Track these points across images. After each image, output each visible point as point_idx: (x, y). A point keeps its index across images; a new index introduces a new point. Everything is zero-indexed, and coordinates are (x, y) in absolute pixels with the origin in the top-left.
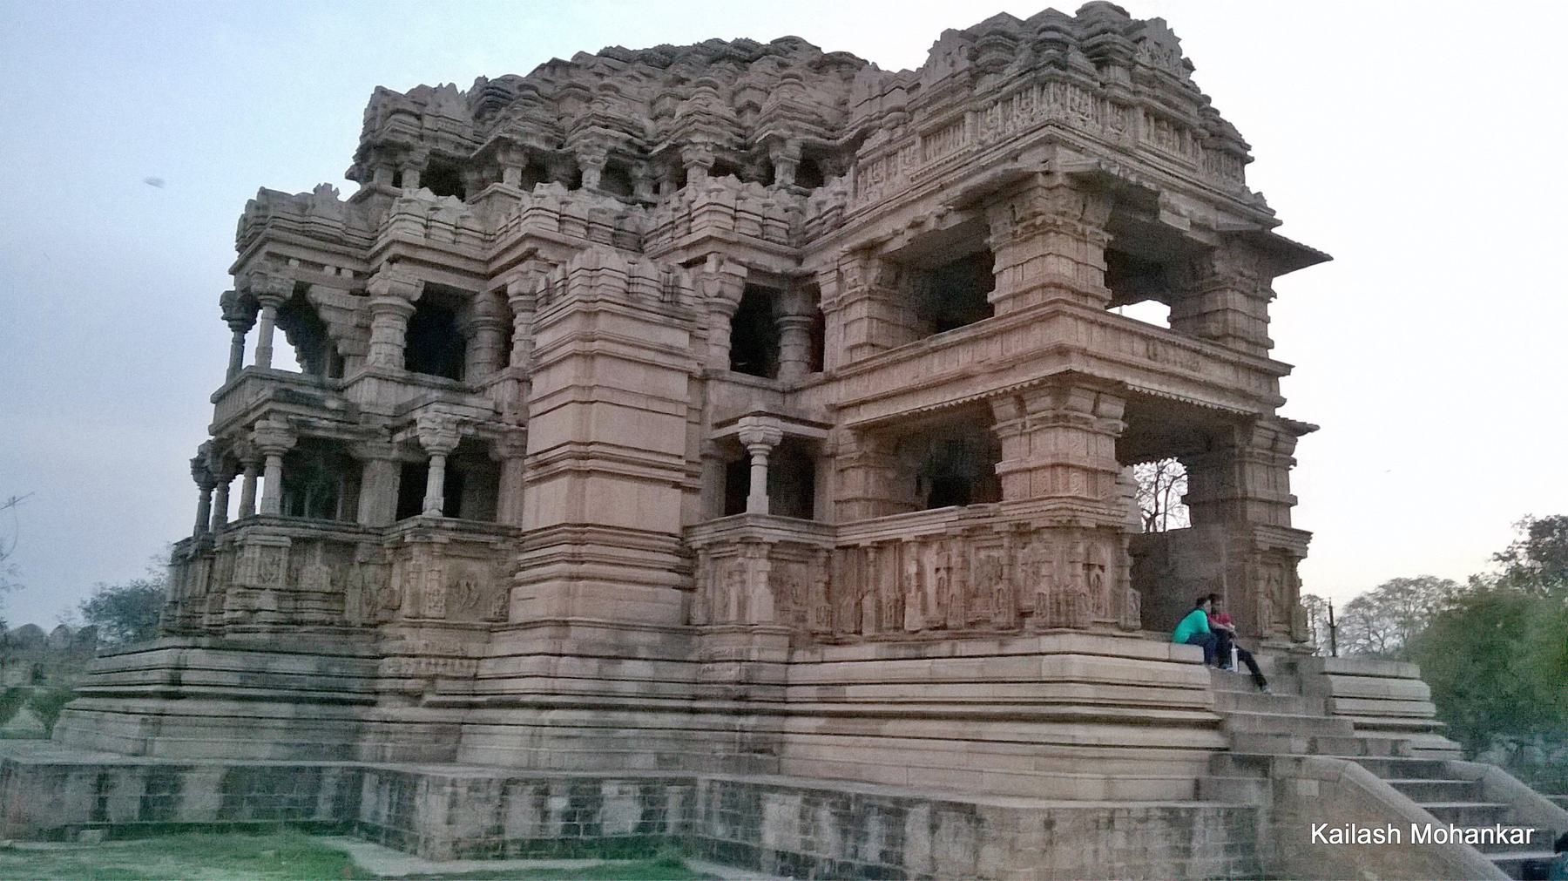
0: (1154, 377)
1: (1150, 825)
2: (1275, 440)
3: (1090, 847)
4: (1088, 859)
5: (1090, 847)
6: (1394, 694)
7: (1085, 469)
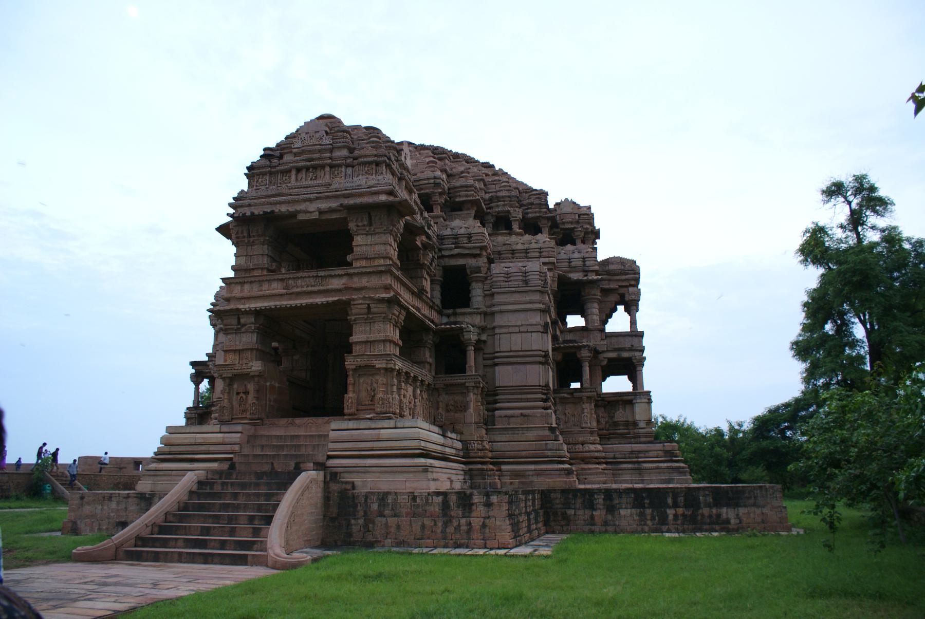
1: (130, 500)
2: (369, 308)
3: (100, 507)
4: (98, 511)
5: (100, 507)
6: (382, 437)
7: (235, 351)
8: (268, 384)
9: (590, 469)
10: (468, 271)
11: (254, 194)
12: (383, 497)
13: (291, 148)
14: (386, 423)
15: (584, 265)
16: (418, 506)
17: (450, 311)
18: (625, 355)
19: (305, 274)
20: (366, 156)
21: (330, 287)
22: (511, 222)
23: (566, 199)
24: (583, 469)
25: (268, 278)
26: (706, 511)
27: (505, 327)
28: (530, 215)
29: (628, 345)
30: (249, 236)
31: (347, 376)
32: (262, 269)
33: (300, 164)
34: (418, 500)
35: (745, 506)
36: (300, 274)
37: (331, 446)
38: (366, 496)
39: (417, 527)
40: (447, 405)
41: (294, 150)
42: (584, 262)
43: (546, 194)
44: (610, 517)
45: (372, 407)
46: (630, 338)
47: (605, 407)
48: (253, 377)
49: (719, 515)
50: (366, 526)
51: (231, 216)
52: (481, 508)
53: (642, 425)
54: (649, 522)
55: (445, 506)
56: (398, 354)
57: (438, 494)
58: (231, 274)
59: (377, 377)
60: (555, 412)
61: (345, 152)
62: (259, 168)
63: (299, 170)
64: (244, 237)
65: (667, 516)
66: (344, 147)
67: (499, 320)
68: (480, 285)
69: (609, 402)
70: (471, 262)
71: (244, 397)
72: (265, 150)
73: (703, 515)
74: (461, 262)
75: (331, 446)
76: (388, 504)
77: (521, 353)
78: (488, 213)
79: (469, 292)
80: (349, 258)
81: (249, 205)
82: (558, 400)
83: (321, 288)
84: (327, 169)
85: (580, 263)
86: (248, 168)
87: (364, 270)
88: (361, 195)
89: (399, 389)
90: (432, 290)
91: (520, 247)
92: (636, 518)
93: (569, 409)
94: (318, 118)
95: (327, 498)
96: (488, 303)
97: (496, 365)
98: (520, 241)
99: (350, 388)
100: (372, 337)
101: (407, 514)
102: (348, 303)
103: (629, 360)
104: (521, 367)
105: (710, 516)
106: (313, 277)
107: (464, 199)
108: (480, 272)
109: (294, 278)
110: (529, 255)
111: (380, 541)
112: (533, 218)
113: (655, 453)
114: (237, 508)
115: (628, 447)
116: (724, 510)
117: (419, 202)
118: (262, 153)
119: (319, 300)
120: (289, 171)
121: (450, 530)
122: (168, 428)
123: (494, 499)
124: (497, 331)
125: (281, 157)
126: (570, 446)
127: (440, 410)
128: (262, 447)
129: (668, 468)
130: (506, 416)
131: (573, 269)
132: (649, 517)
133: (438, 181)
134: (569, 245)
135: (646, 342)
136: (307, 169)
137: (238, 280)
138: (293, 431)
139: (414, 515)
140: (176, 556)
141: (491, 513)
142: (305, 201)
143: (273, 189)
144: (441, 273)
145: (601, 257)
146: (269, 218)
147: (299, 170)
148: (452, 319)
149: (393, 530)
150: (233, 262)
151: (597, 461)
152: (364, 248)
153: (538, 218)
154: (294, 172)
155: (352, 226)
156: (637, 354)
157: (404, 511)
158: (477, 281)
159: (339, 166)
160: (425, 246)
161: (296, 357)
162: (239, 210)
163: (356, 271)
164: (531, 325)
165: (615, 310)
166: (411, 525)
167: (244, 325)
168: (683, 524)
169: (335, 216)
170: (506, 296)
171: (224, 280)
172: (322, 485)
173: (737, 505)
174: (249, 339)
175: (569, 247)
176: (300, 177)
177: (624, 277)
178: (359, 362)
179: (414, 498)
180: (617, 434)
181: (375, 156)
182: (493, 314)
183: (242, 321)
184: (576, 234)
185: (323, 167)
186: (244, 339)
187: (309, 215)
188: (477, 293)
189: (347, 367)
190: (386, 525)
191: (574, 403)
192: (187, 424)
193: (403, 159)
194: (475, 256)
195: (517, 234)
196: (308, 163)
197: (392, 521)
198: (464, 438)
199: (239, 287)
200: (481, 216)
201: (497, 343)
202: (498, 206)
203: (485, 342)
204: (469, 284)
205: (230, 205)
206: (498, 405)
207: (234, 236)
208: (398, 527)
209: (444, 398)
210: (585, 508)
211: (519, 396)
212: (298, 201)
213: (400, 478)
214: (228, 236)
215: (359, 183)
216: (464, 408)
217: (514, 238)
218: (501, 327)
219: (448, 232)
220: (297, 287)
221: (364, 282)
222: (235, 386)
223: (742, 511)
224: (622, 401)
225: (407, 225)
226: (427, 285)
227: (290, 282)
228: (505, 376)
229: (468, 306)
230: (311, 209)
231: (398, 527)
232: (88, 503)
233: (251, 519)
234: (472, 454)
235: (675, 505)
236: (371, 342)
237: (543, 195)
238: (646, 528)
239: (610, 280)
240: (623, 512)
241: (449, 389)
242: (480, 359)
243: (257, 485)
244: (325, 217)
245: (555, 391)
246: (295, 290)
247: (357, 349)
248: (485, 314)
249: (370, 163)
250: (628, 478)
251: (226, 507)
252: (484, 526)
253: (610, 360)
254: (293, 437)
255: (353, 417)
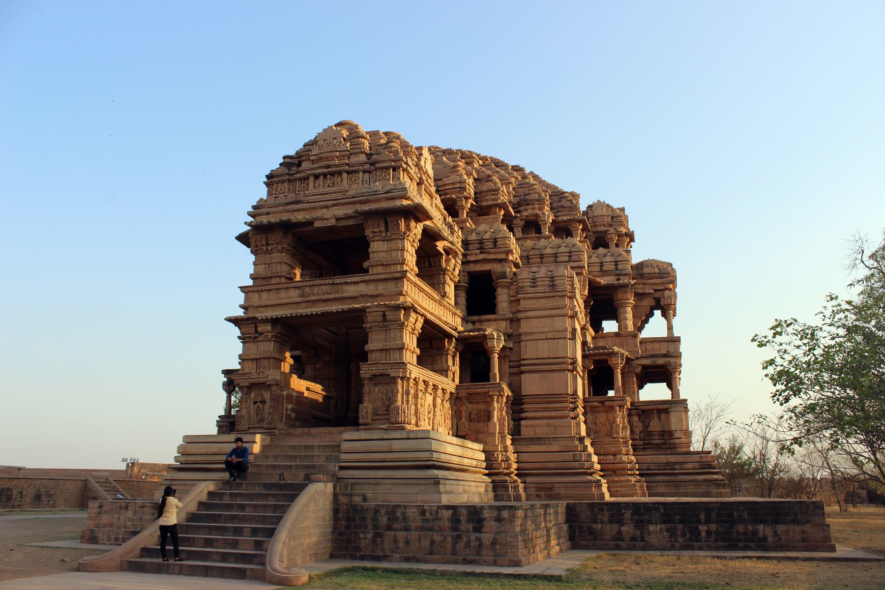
0: (303, 305)
1: (145, 509)
3: (117, 516)
7: (252, 359)
8: (285, 393)
9: (622, 481)
10: (493, 276)
11: (272, 201)
12: (392, 511)
13: (309, 155)
14: (398, 434)
15: (617, 269)
16: (427, 520)
17: (476, 318)
18: (660, 361)
19: (322, 282)
20: (383, 161)
21: (346, 295)
22: (540, 226)
23: (599, 201)
24: (614, 482)
25: (285, 286)
26: (740, 528)
27: (531, 334)
28: (560, 218)
29: (664, 352)
30: (268, 245)
31: (363, 385)
32: (280, 277)
33: (317, 171)
34: (427, 515)
35: (784, 522)
36: (317, 282)
37: (343, 456)
38: (376, 511)
39: (426, 544)
40: (470, 415)
41: (312, 158)
42: (616, 265)
43: (578, 196)
44: (638, 532)
45: (387, 417)
46: (666, 344)
47: (639, 416)
48: (269, 386)
49: (755, 532)
50: (374, 541)
51: (249, 224)
52: (493, 523)
53: (677, 435)
54: (680, 540)
55: (455, 520)
56: (415, 362)
57: (448, 507)
58: (250, 282)
59: (392, 386)
60: (585, 422)
61: (363, 158)
62: (278, 176)
63: (316, 177)
64: (262, 245)
65: (699, 532)
66: (362, 153)
67: (525, 327)
68: (506, 291)
69: (643, 411)
70: (496, 268)
71: (261, 406)
72: (284, 158)
73: (738, 533)
74: (486, 267)
75: (343, 456)
76: (398, 518)
77: (548, 361)
78: (516, 217)
79: (495, 298)
80: (366, 264)
81: (268, 213)
82: (588, 409)
83: (337, 296)
84: (345, 175)
85: (613, 267)
86: (267, 176)
87: (379, 277)
88: (378, 201)
89: (416, 396)
90: (456, 296)
91: (549, 251)
92: (666, 534)
93: (601, 417)
94: (336, 126)
95: (336, 511)
96: (514, 309)
97: (523, 372)
98: (549, 243)
99: (366, 398)
100: (389, 345)
101: (417, 529)
102: (363, 310)
103: (664, 366)
104: (548, 375)
105: (745, 533)
106: (329, 284)
107: (491, 203)
108: (506, 278)
109: (311, 286)
110: (559, 259)
111: (388, 556)
112: (564, 221)
113: (690, 465)
114: (243, 519)
115: (662, 459)
116: (761, 527)
117: (442, 207)
118: (282, 161)
119: (334, 307)
120: (307, 178)
121: (461, 545)
122: (185, 437)
123: (505, 514)
124: (523, 338)
125: (299, 165)
126: (601, 457)
127: (463, 420)
128: (276, 457)
129: (705, 480)
130: (532, 426)
131: (603, 273)
132: (679, 533)
133: (462, 185)
134: (601, 248)
135: (683, 348)
136: (325, 175)
137: (256, 289)
138: (308, 441)
139: (421, 529)
140: (177, 568)
141: (502, 529)
142: (322, 208)
143: (291, 197)
144: (466, 279)
145: (636, 259)
146: (286, 227)
147: (316, 177)
148: (477, 326)
149: (401, 545)
150: (251, 270)
151: (629, 472)
152: (382, 255)
153: (569, 220)
154: (311, 179)
155: (368, 232)
156: (672, 360)
157: (413, 525)
158: (503, 287)
159: (357, 172)
160: (448, 251)
161: (318, 366)
162: (259, 219)
163: (372, 277)
164: (559, 331)
165: (651, 315)
166: (420, 540)
167: (261, 334)
168: (716, 540)
169: (351, 222)
170: (531, 301)
171: (242, 289)
172: (331, 497)
173: (776, 522)
174: (268, 347)
175: (601, 250)
176: (317, 183)
177: (659, 281)
178: (375, 370)
179: (423, 512)
180: (652, 444)
181: (392, 161)
182: (519, 320)
183: (260, 329)
184: (609, 236)
185: (340, 173)
186: (262, 348)
187: (325, 222)
188: (503, 298)
189: (362, 376)
190: (395, 541)
191: (606, 412)
192: (219, 432)
193: (422, 163)
194: (500, 261)
195: (548, 238)
196: (325, 170)
197: (401, 535)
198: (488, 448)
199: (256, 295)
200: (508, 220)
201: (523, 350)
202: (526, 210)
203: (511, 349)
204: (495, 290)
205: (250, 214)
206: (524, 415)
207: (252, 244)
208: (407, 542)
209: (466, 408)
210: (611, 522)
211: (546, 405)
212: (315, 208)
213: (410, 490)
214: (248, 245)
215: (375, 189)
216: (489, 417)
217: (543, 242)
218: (527, 334)
219: (473, 237)
220: (313, 294)
221: (380, 288)
222: (253, 395)
223: (781, 528)
224: (658, 410)
225: (426, 232)
226: (450, 290)
227: (307, 289)
228: (532, 384)
229: (494, 312)
230: (325, 217)
231: (407, 542)
232: (106, 512)
233: (255, 532)
234: (494, 466)
235: (708, 521)
236: (386, 350)
237: (575, 196)
238: (677, 545)
239: (644, 284)
240: (652, 528)
241: (471, 398)
242: (506, 367)
243: (265, 496)
244: (342, 223)
245: (585, 400)
246: (312, 298)
247: (372, 357)
248: (511, 320)
249: (388, 168)
250: (661, 490)
251: (232, 518)
252: (494, 543)
253: (644, 367)
254: (307, 447)
255: (367, 427)
